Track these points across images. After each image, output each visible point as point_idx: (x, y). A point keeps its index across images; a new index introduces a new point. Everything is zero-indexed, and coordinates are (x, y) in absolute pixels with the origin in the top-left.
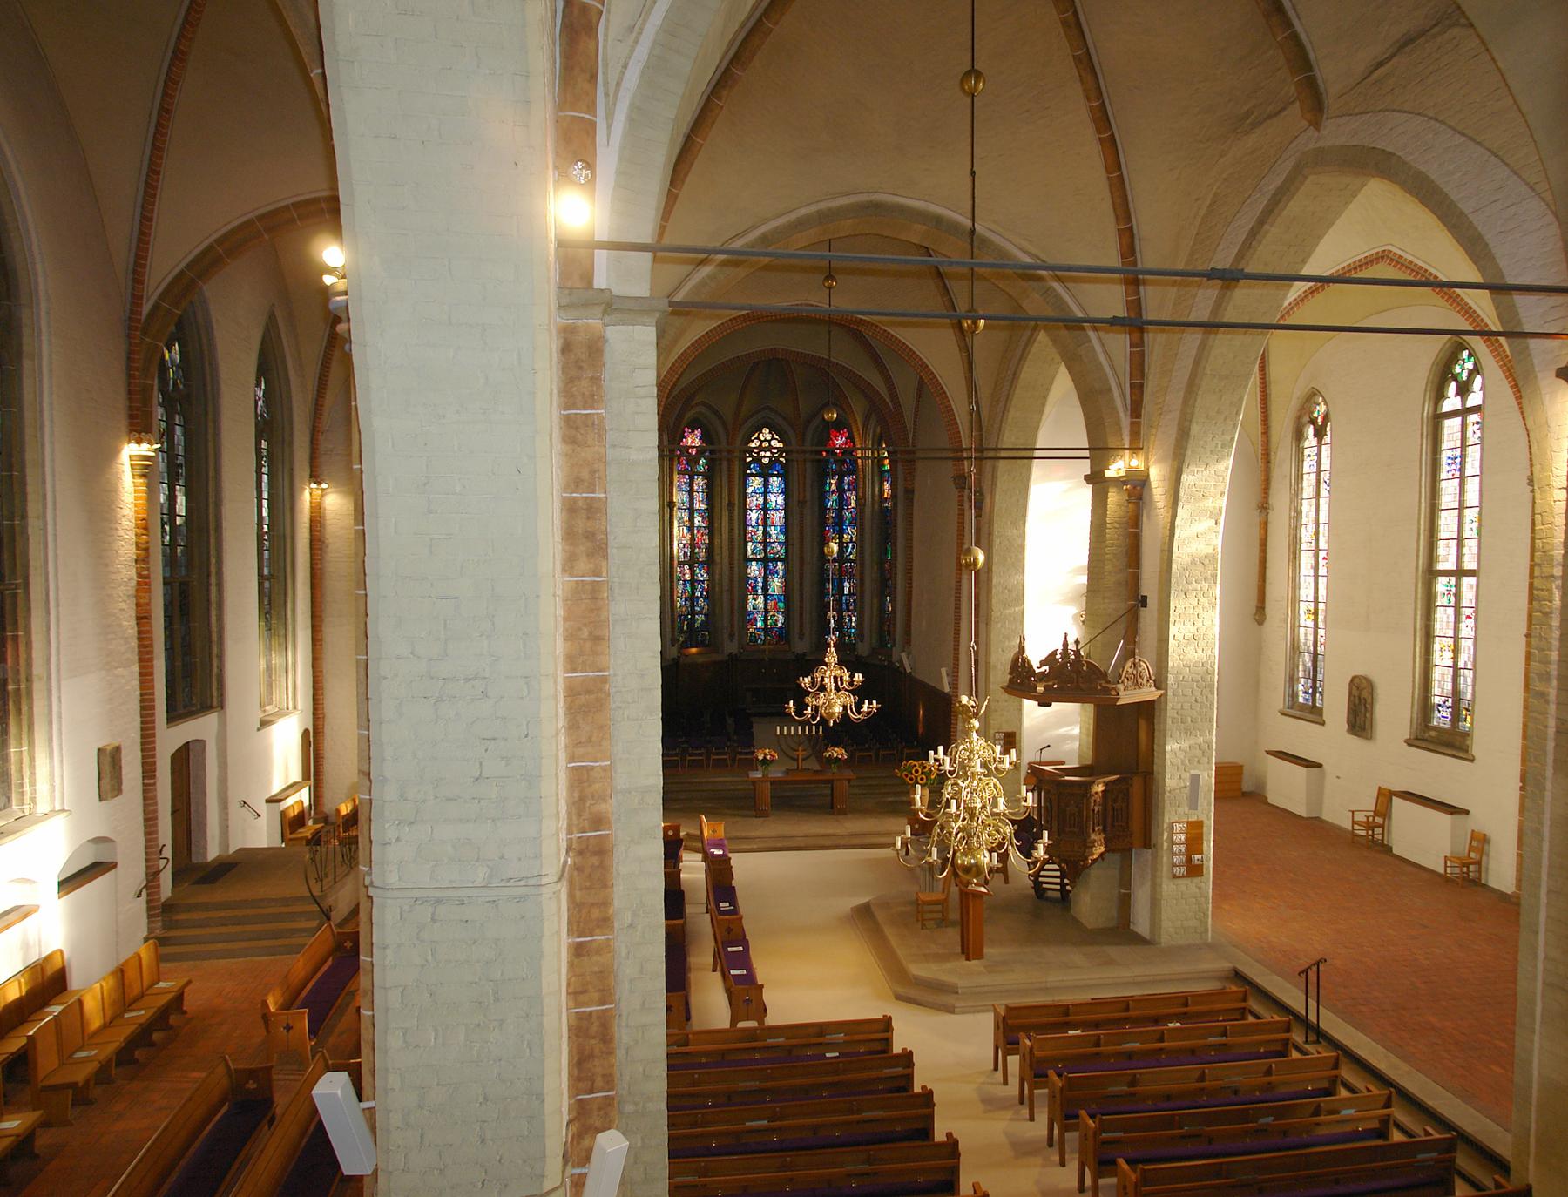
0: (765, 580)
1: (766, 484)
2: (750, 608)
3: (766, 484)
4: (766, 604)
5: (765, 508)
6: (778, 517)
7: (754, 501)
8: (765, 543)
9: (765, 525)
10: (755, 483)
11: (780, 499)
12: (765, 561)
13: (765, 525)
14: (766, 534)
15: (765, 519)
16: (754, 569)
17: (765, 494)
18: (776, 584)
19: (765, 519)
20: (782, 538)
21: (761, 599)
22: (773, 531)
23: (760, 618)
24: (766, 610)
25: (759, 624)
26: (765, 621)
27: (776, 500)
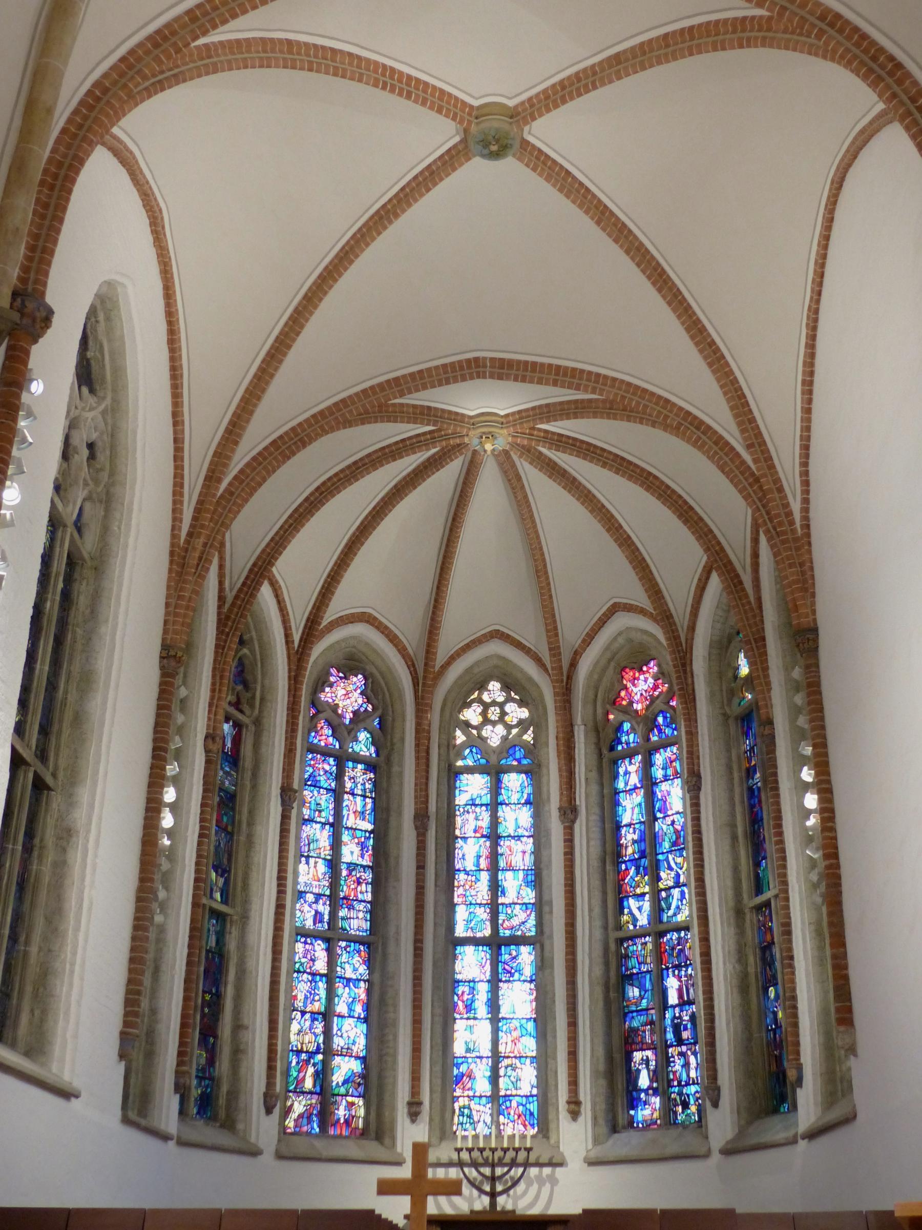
0: (495, 982)
1: (496, 788)
2: (459, 1049)
3: (496, 788)
4: (495, 1042)
5: (494, 837)
6: (518, 854)
7: (470, 823)
8: (494, 909)
9: (494, 869)
10: (474, 786)
11: (525, 816)
12: (496, 944)
13: (494, 869)
14: (495, 887)
15: (494, 856)
16: (471, 964)
17: (494, 805)
18: (518, 1000)
19: (494, 856)
20: (529, 895)
21: (483, 1030)
22: (512, 883)
23: (482, 1071)
24: (496, 1057)
25: (483, 1086)
26: (494, 1079)
27: (516, 818)
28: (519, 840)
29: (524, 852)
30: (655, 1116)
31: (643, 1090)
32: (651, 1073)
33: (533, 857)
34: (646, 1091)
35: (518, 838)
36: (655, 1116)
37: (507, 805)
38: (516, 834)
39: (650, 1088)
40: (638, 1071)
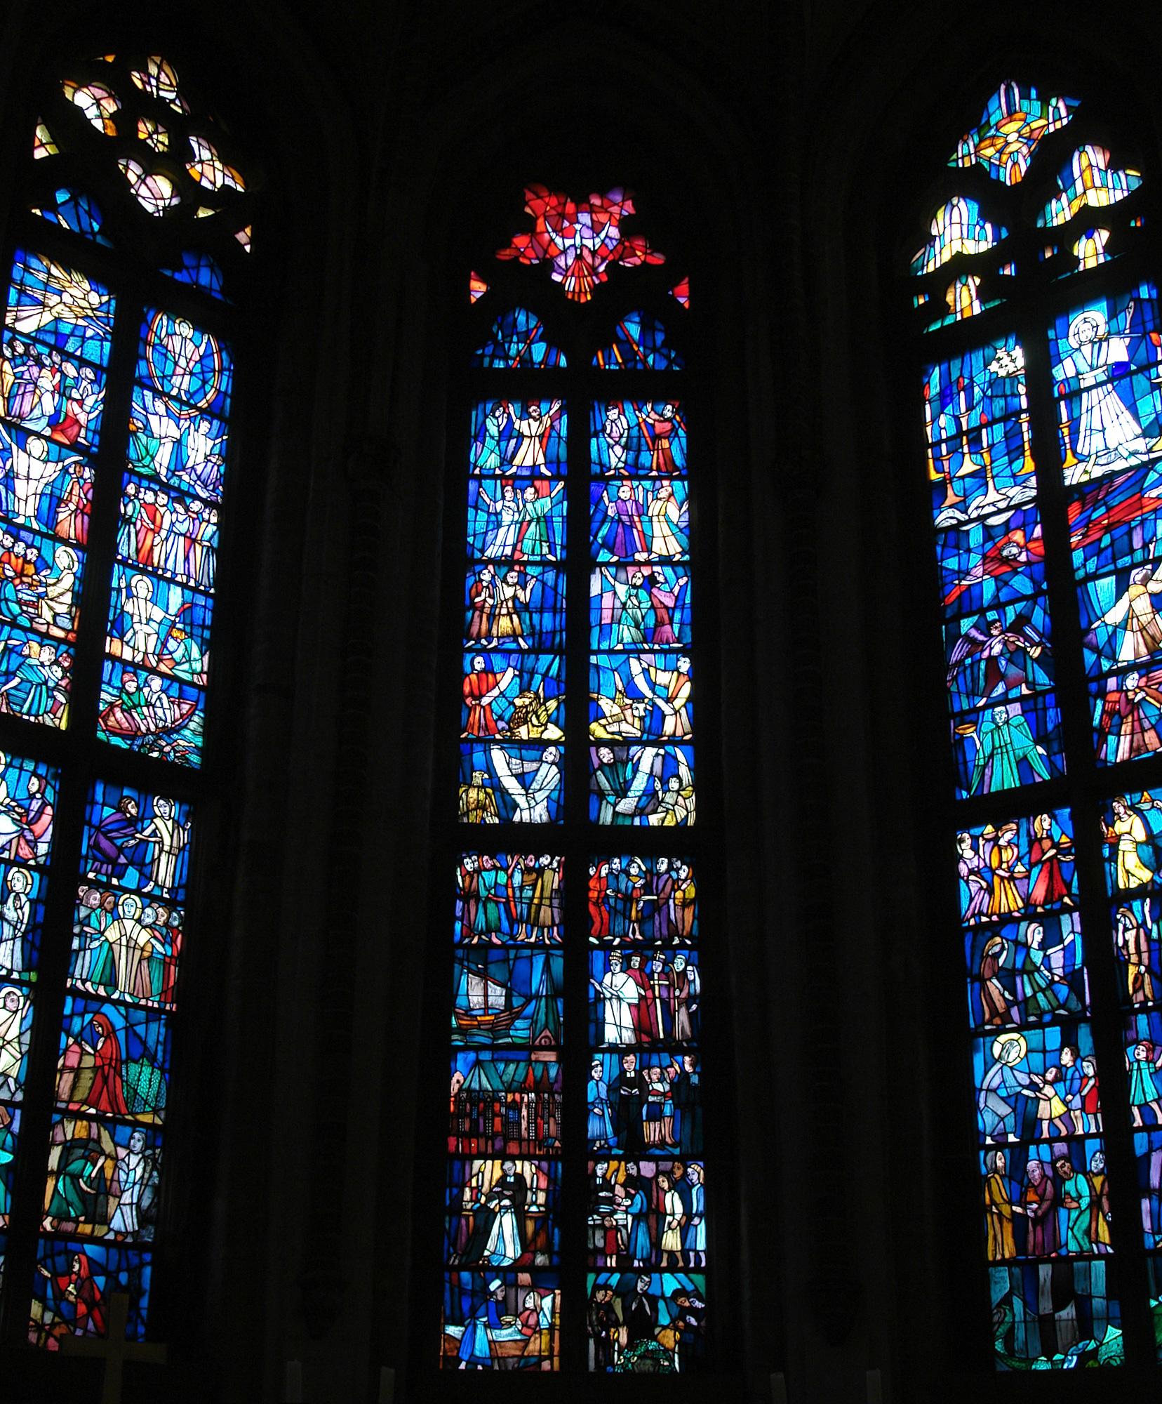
1: (128, 338)
3: (128, 338)
11: (202, 445)
27: (180, 441)
28: (180, 500)
29: (191, 540)
30: (533, 1347)
31: (499, 1271)
32: (530, 1226)
33: (213, 561)
34: (508, 1274)
35: (180, 496)
36: (533, 1347)
37: (158, 394)
38: (174, 481)
39: (518, 1266)
40: (486, 1217)
